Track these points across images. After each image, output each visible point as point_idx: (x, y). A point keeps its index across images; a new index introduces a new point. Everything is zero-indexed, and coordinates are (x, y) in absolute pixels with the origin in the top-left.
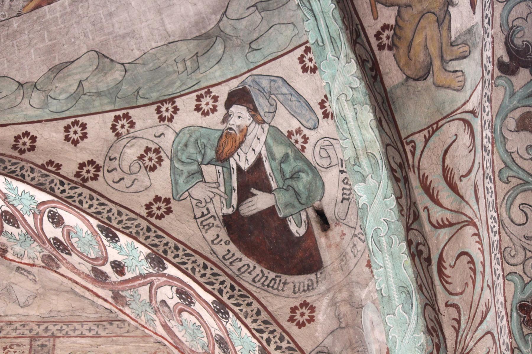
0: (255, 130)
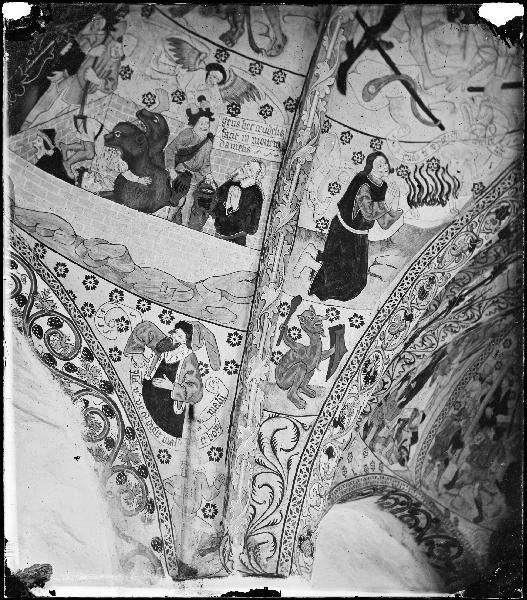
0: (183, 348)
